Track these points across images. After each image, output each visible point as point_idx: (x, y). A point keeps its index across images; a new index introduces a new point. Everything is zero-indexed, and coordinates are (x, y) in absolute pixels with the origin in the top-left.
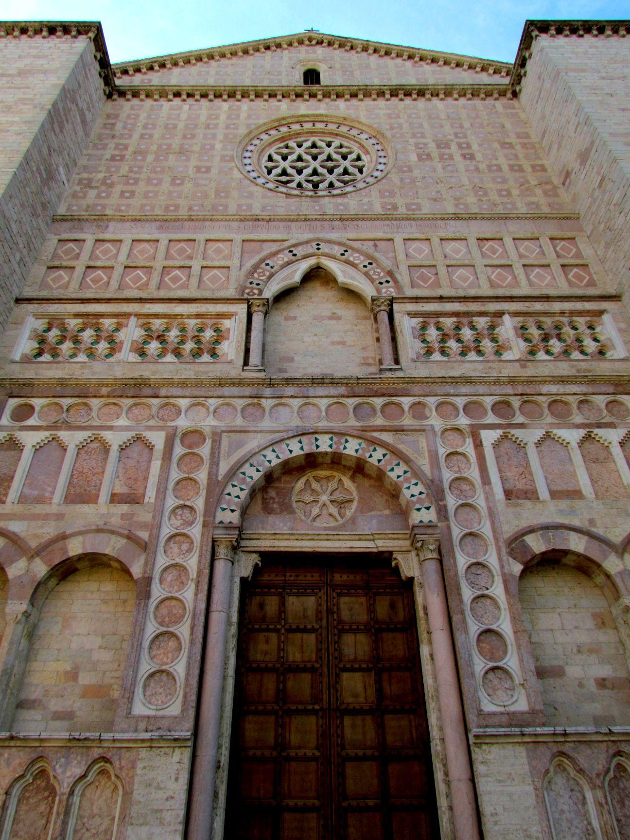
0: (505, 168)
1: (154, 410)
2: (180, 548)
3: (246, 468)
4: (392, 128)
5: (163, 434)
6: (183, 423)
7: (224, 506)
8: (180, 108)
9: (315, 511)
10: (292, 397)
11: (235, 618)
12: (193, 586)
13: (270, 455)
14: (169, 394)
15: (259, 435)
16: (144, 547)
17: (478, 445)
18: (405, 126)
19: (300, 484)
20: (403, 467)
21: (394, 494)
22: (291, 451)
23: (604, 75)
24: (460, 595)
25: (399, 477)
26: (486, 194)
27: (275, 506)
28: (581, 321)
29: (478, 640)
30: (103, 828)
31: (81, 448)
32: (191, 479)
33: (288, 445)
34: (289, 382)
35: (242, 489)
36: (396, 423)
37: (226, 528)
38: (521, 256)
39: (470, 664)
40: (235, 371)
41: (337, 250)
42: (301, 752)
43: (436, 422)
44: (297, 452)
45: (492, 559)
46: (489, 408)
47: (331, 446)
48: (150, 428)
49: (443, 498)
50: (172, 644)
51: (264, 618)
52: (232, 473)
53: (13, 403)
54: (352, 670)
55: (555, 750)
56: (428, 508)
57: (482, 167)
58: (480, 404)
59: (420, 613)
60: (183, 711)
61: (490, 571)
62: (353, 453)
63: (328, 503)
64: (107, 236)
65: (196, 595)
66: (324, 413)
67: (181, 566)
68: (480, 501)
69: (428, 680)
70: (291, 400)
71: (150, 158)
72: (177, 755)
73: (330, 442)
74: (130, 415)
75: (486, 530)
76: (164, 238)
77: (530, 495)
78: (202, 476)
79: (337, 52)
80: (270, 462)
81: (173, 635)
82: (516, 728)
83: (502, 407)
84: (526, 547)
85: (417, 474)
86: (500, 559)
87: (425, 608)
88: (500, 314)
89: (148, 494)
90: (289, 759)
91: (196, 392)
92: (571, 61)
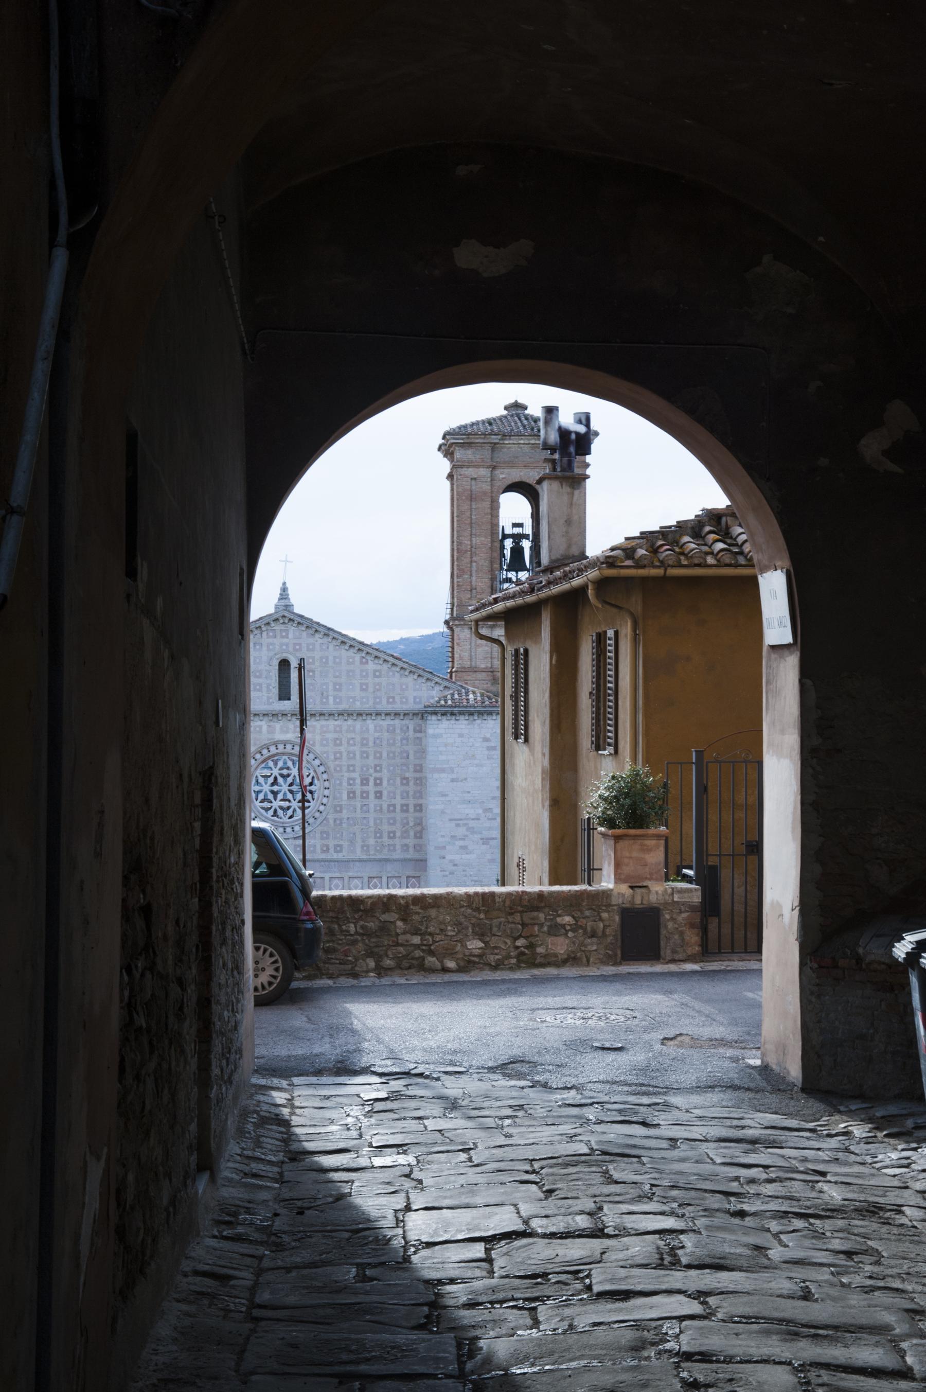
0: (398, 808)
4: (336, 759)
18: (345, 754)
23: (454, 776)
26: (381, 837)
79: (304, 634)
92: (442, 758)
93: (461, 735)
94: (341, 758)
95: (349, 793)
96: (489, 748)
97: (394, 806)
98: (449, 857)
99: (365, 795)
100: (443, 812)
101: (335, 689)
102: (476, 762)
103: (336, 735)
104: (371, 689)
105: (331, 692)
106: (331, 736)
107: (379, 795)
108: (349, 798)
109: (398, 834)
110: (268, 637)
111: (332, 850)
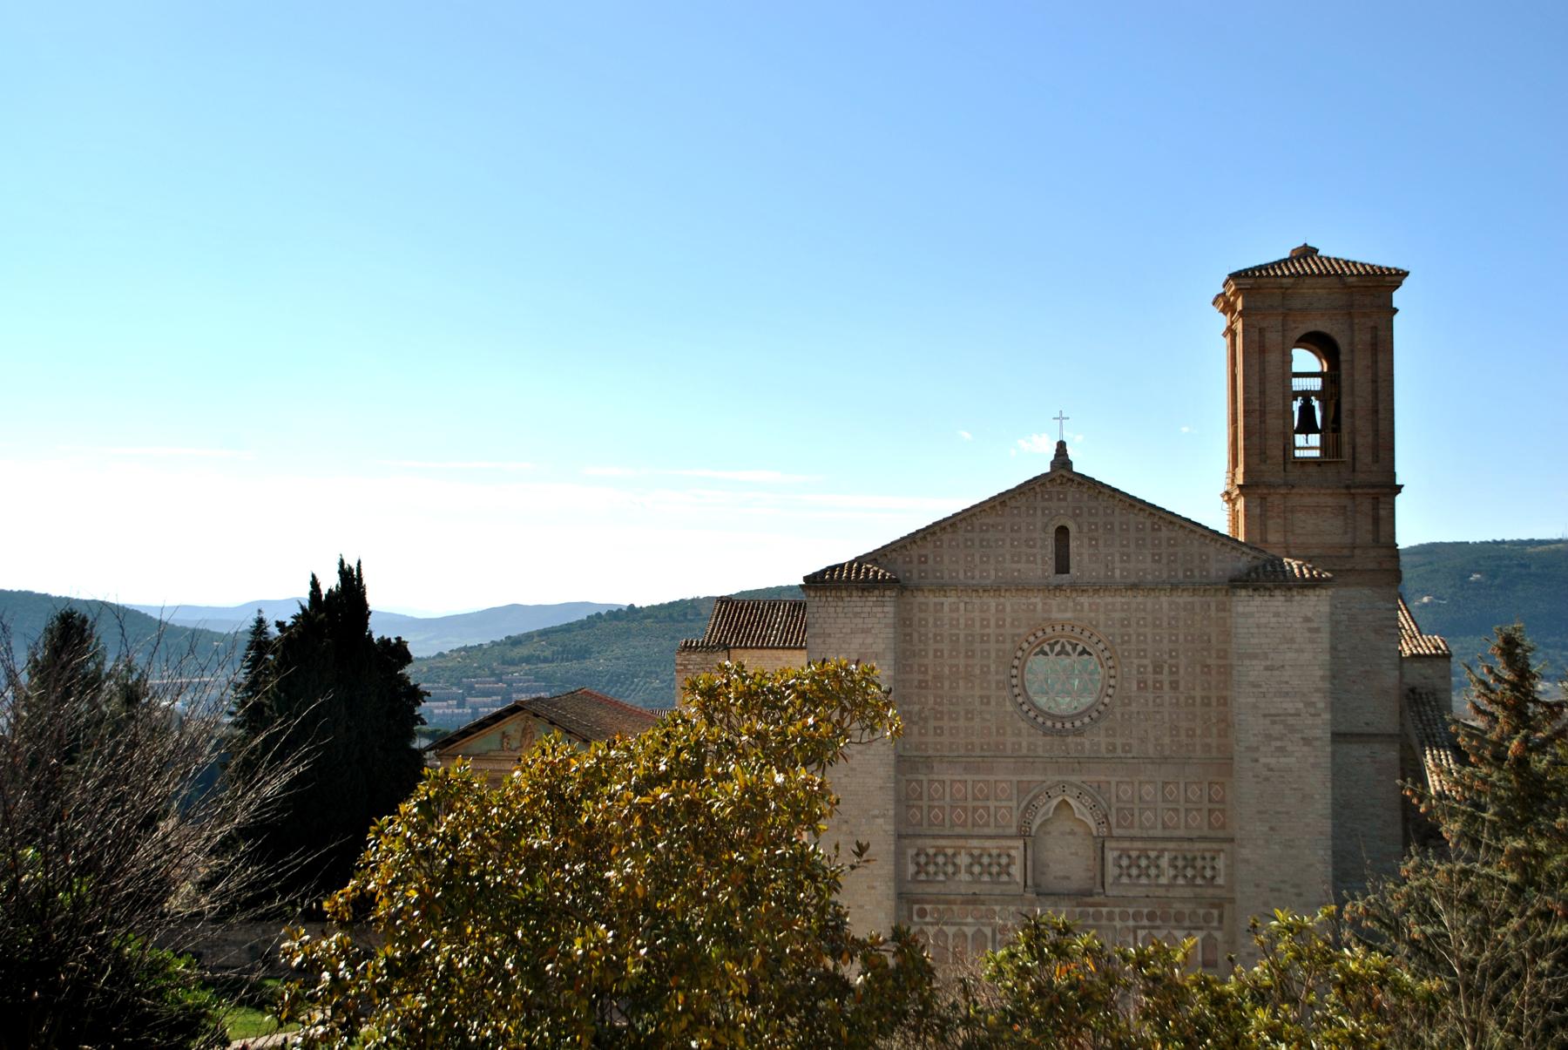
4: (1123, 642)
8: (958, 609)
18: (1134, 637)
26: (1178, 735)
28: (1208, 855)
31: (955, 936)
38: (1187, 800)
41: (1076, 792)
43: (1118, 924)
53: (916, 907)
57: (1182, 699)
64: (935, 777)
71: (947, 684)
76: (968, 777)
88: (1163, 851)
92: (1254, 641)
93: (1277, 615)
94: (1129, 641)
95: (1139, 683)
96: (1311, 630)
97: (1193, 698)
98: (1262, 760)
99: (1157, 686)
100: (1255, 706)
101: (1122, 561)
102: (1295, 646)
103: (1123, 615)
104: (1164, 561)
105: (1118, 565)
106: (1116, 615)
107: (1174, 686)
108: (1139, 688)
109: (1198, 732)
110: (1044, 500)
111: (1119, 750)
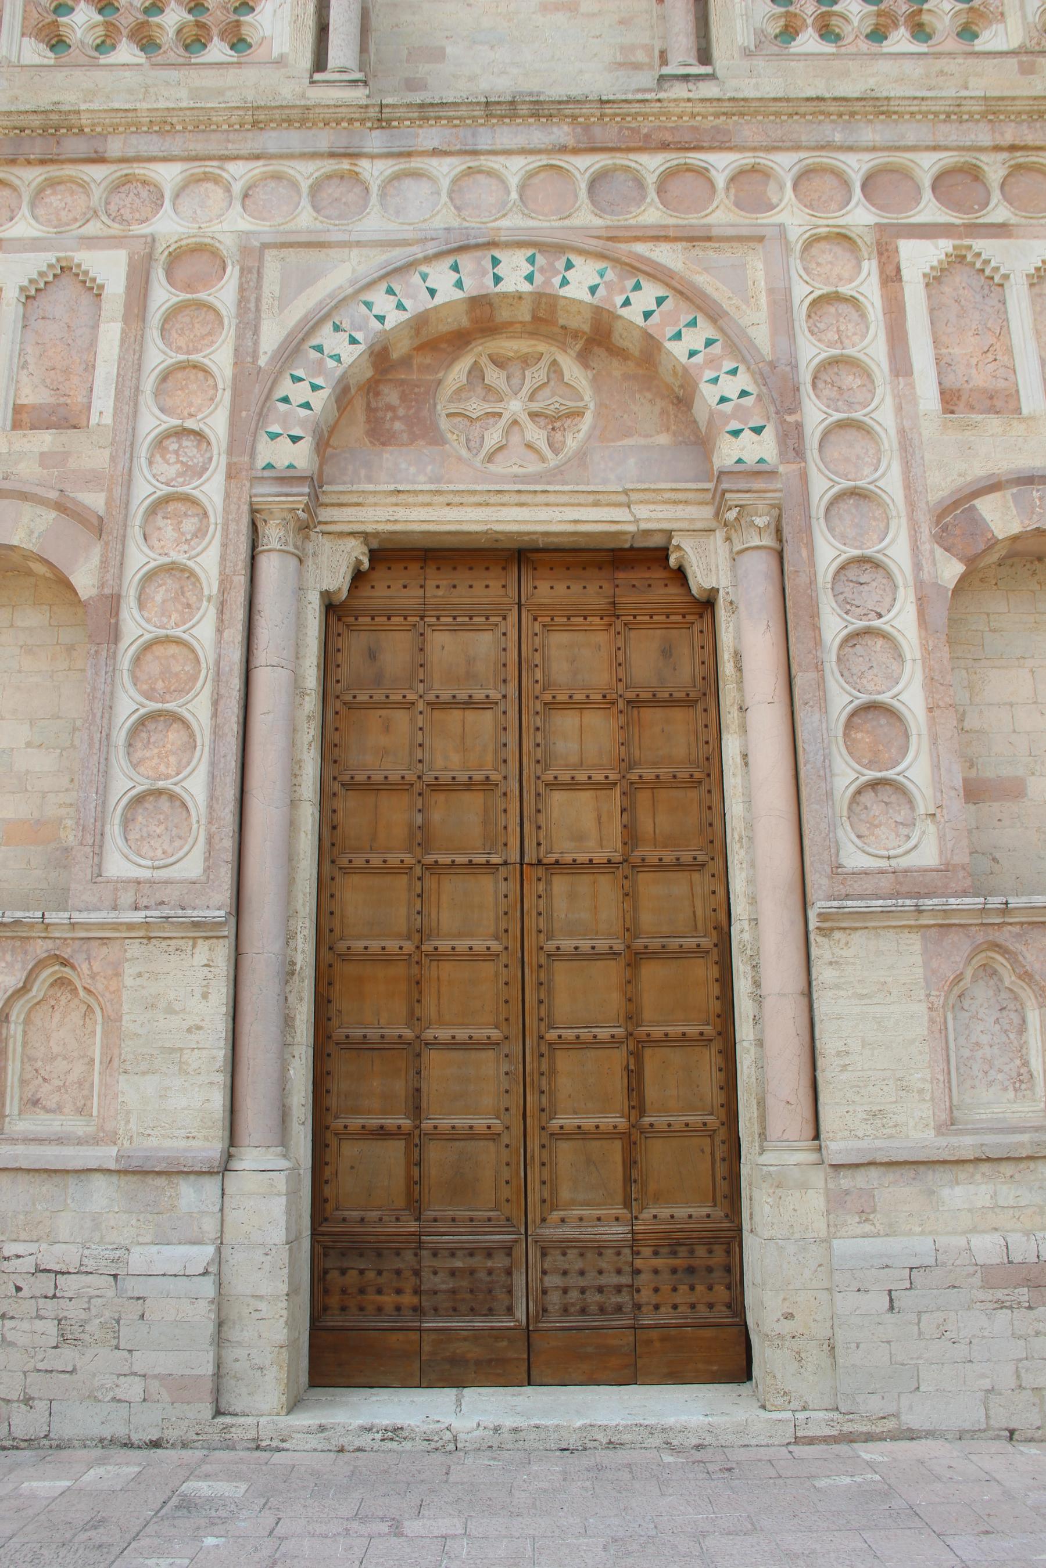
1: (97, 194)
2: (178, 528)
3: (326, 337)
5: (120, 257)
6: (169, 226)
7: (276, 428)
9: (493, 437)
10: (436, 152)
11: (311, 679)
12: (212, 613)
13: (383, 303)
14: (131, 153)
15: (355, 252)
16: (97, 527)
17: (891, 277)
19: (458, 373)
20: (705, 330)
21: (680, 398)
22: (432, 292)
24: (816, 628)
25: (692, 354)
27: (398, 426)
29: (849, 725)
30: (73, 1077)
32: (196, 366)
33: (424, 277)
34: (428, 112)
35: (315, 388)
36: (693, 219)
37: (281, 480)
39: (826, 773)
40: (291, 86)
42: (462, 945)
43: (792, 217)
44: (447, 292)
45: (897, 551)
46: (927, 182)
47: (530, 278)
48: (90, 242)
49: (795, 407)
50: (175, 736)
51: (378, 680)
52: (293, 348)
54: (573, 785)
55: (980, 938)
56: (758, 430)
58: (904, 174)
59: (727, 668)
60: (207, 869)
61: (889, 576)
62: (585, 296)
63: (524, 418)
65: (219, 631)
66: (514, 195)
67: (183, 569)
68: (883, 416)
69: (735, 808)
70: (434, 162)
72: (202, 952)
73: (527, 268)
74: (40, 211)
75: (891, 484)
77: (1001, 402)
78: (220, 358)
80: (381, 319)
81: (175, 718)
82: (908, 903)
83: (959, 182)
84: (975, 522)
85: (736, 346)
86: (915, 549)
87: (738, 656)
89: (97, 405)
90: (437, 956)
91: (198, 146)
